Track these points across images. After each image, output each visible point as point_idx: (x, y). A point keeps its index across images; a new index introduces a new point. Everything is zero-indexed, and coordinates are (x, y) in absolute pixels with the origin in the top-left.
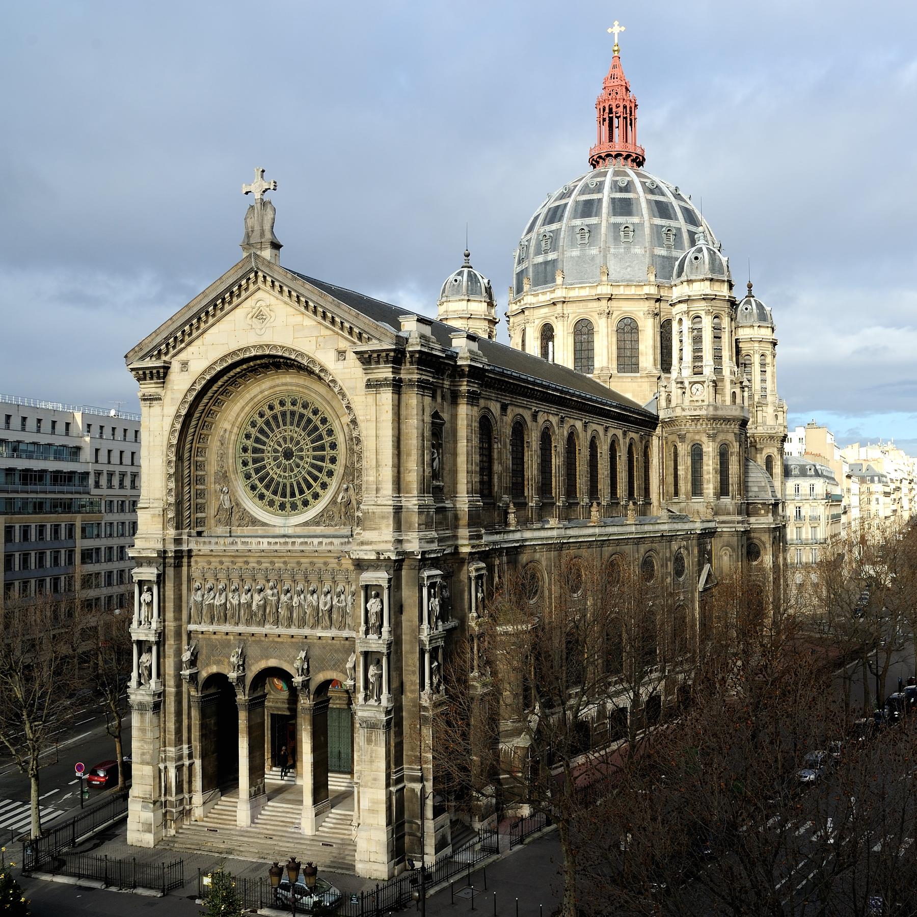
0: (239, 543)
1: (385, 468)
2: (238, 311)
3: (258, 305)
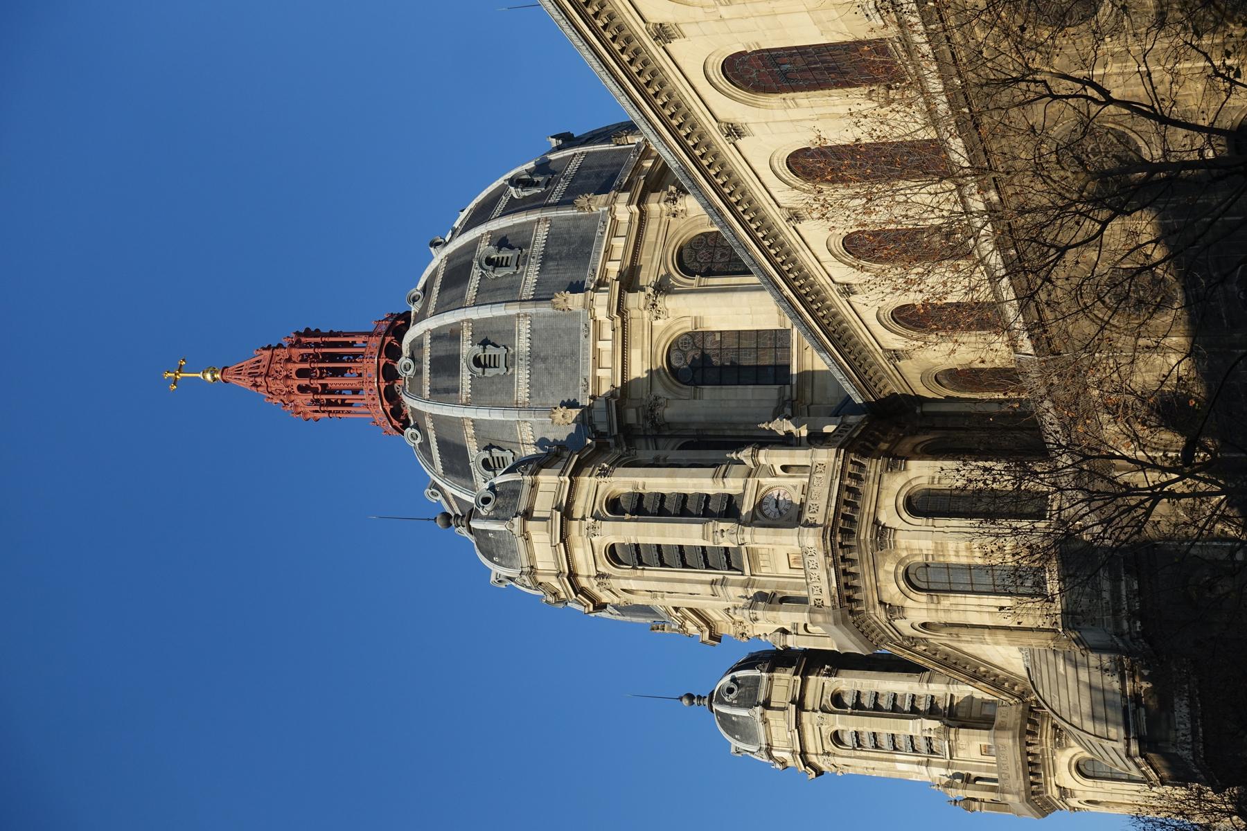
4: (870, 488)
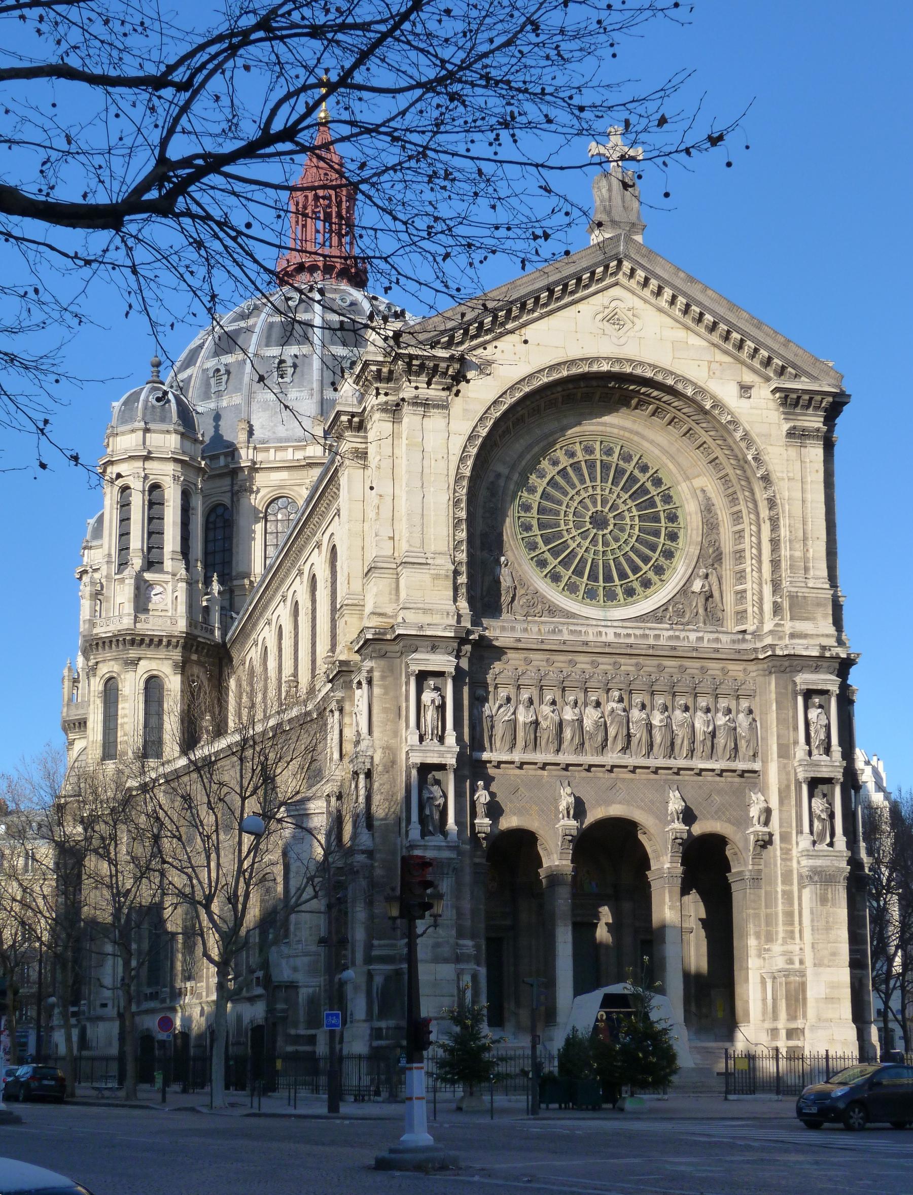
0: (565, 631)
1: (818, 542)
2: (580, 306)
3: (613, 305)
4: (162, 653)
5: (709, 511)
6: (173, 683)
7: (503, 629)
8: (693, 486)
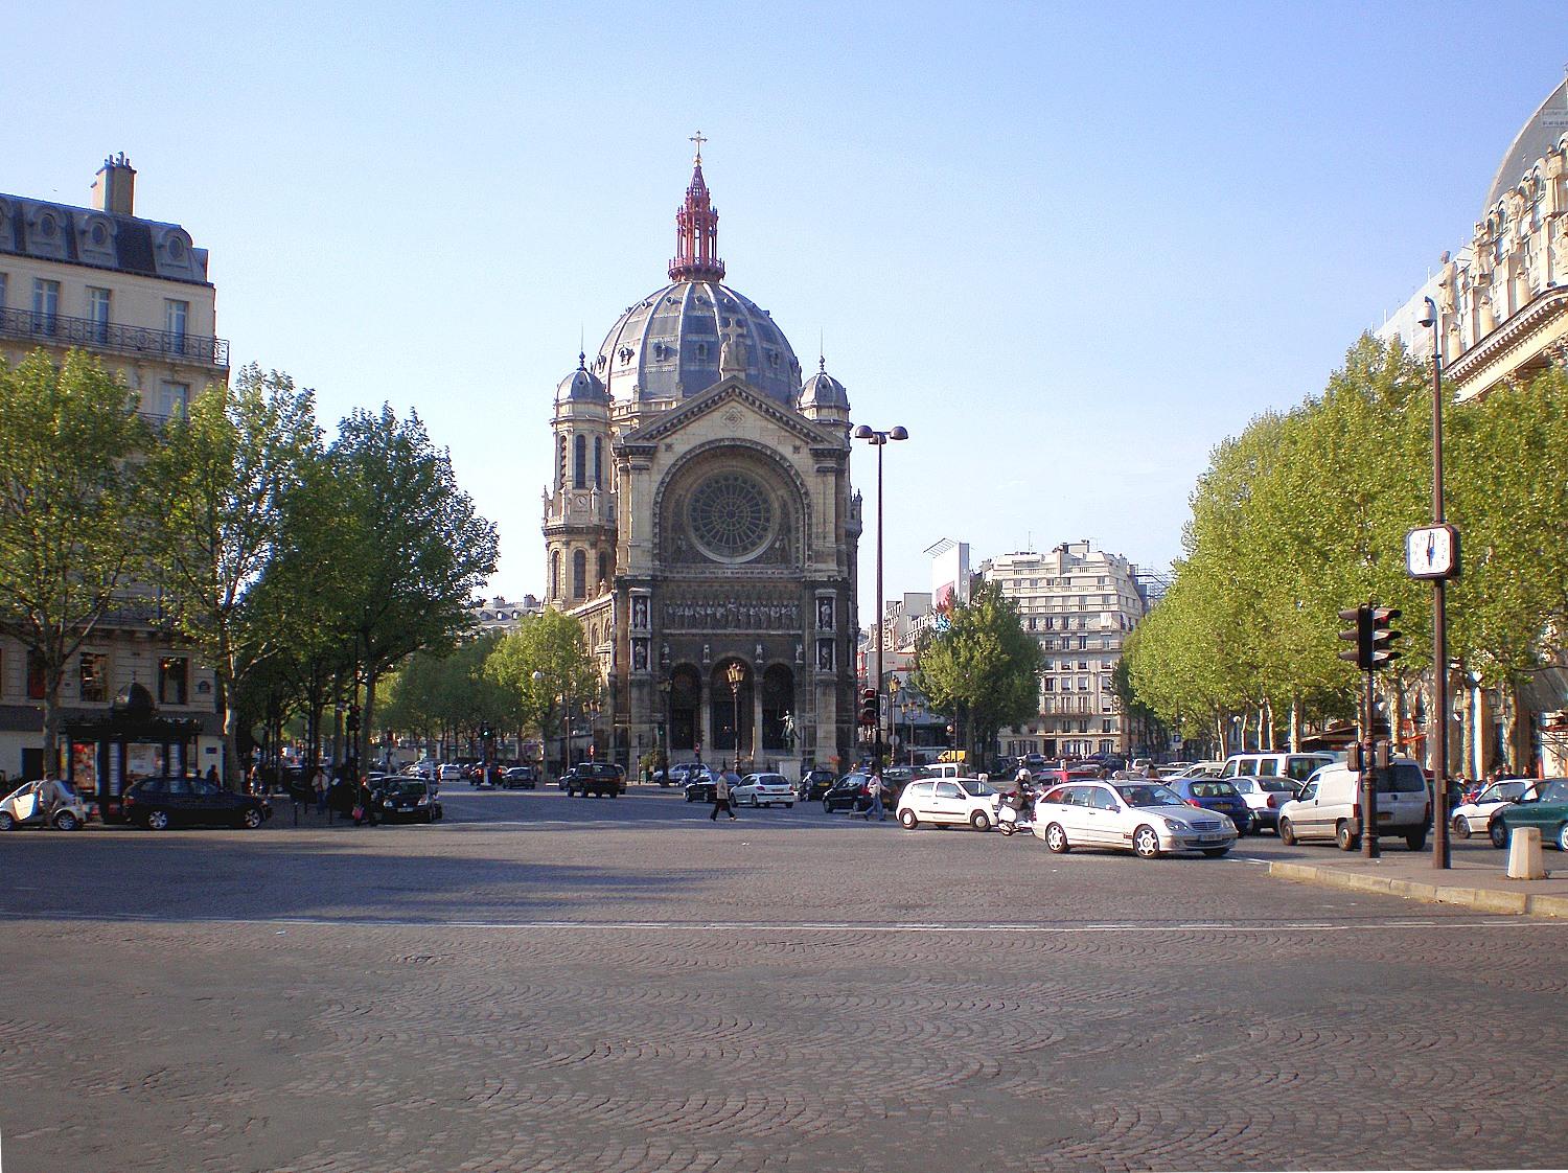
4: (584, 537)
5: (784, 506)
6: (591, 555)
7: (678, 572)
8: (777, 495)
